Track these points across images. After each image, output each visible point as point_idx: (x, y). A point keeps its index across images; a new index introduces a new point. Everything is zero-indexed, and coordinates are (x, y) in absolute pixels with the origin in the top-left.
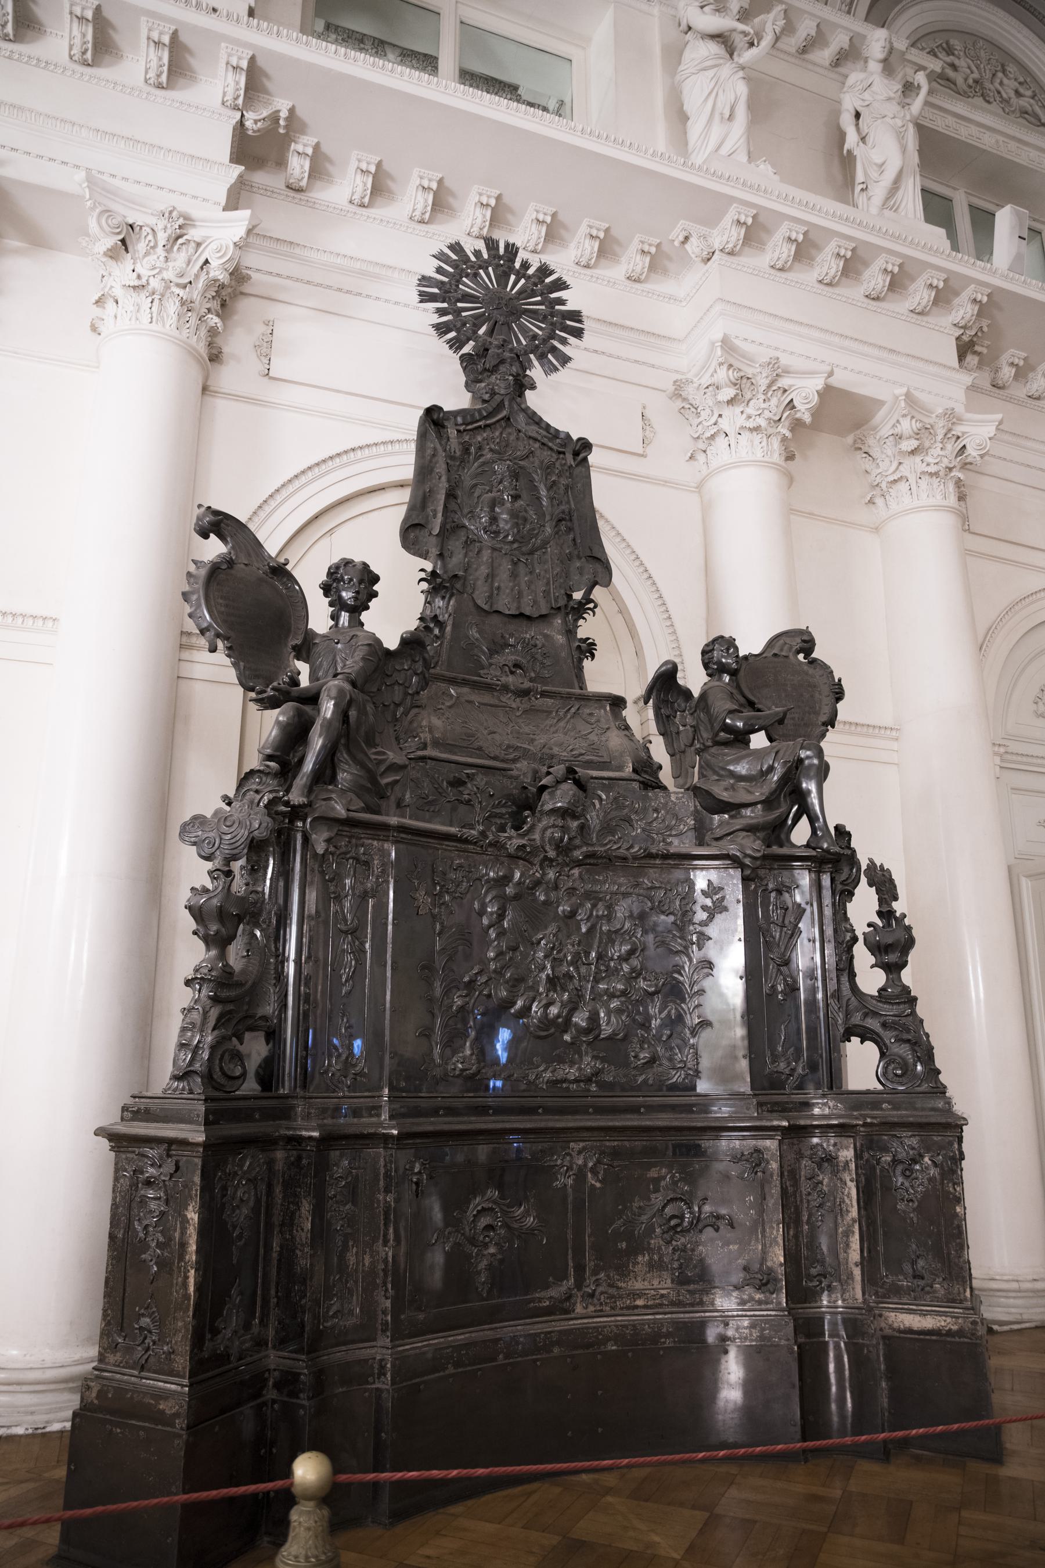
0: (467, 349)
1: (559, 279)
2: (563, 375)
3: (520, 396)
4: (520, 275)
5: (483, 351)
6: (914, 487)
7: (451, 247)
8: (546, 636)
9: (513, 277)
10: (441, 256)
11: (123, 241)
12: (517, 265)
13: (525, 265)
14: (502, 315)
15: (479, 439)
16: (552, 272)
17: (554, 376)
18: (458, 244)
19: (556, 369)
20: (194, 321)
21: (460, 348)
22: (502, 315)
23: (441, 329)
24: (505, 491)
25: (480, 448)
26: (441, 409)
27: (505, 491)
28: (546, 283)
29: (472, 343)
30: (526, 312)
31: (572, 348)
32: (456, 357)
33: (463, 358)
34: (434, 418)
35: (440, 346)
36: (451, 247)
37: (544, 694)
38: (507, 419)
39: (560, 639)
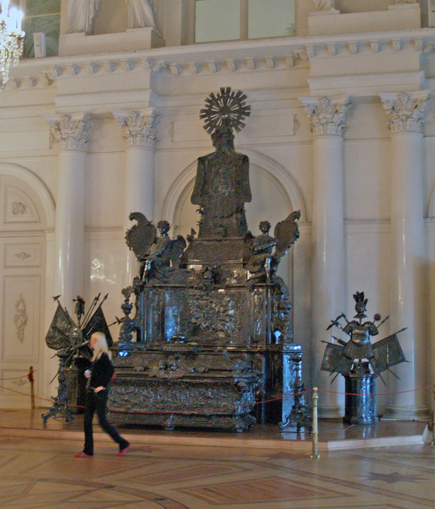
0: (213, 132)
1: (244, 95)
5: (217, 131)
8: (231, 221)
10: (208, 100)
13: (233, 94)
19: (240, 130)
20: (145, 138)
21: (211, 132)
24: (223, 177)
25: (215, 165)
27: (223, 177)
28: (239, 97)
29: (215, 129)
32: (209, 136)
33: (213, 136)
37: (225, 240)
39: (235, 221)
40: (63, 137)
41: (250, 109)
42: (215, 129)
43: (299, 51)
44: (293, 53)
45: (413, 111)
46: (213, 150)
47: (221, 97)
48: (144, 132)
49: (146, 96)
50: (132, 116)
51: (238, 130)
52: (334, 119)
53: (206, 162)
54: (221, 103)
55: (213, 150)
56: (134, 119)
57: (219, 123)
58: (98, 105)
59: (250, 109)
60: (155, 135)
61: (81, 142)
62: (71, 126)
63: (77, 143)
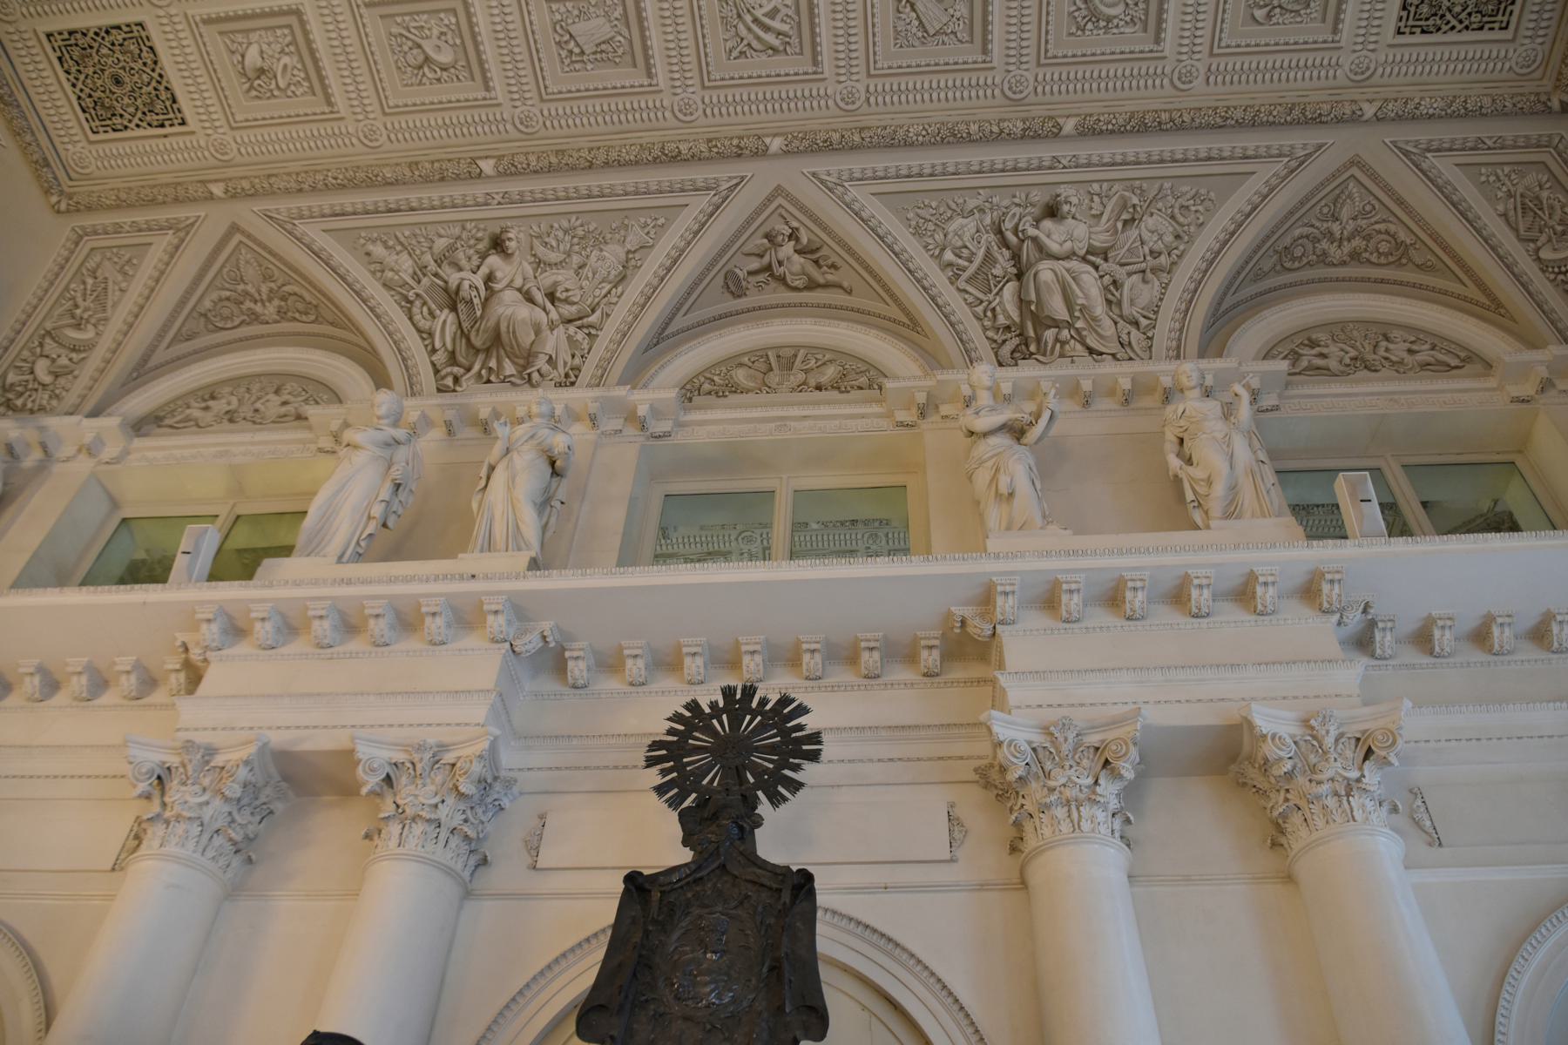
2: (795, 802)
3: (742, 839)
4: (754, 715)
5: (701, 804)
6: (1308, 816)
7: (687, 707)
9: (715, 722)
10: (677, 718)
11: (388, 776)
12: (754, 705)
13: (763, 702)
14: (732, 759)
15: (689, 895)
16: (793, 700)
17: (783, 807)
18: (695, 702)
19: (785, 799)
20: (444, 835)
22: (732, 759)
23: (660, 790)
26: (640, 874)
28: (785, 712)
29: (694, 795)
30: (757, 749)
31: (808, 773)
32: (675, 815)
33: (684, 817)
34: (635, 883)
35: (657, 804)
36: (687, 707)
38: (723, 867)
40: (168, 814)
41: (820, 743)
42: (694, 795)
43: (967, 611)
44: (949, 614)
45: (1361, 769)
46: (685, 856)
47: (724, 710)
48: (443, 813)
49: (478, 711)
50: (416, 757)
51: (776, 800)
52: (1098, 789)
53: (656, 895)
54: (722, 725)
55: (685, 856)
56: (419, 766)
57: (712, 779)
58: (311, 730)
59: (820, 743)
60: (479, 820)
61: (218, 840)
62: (206, 782)
63: (206, 837)
